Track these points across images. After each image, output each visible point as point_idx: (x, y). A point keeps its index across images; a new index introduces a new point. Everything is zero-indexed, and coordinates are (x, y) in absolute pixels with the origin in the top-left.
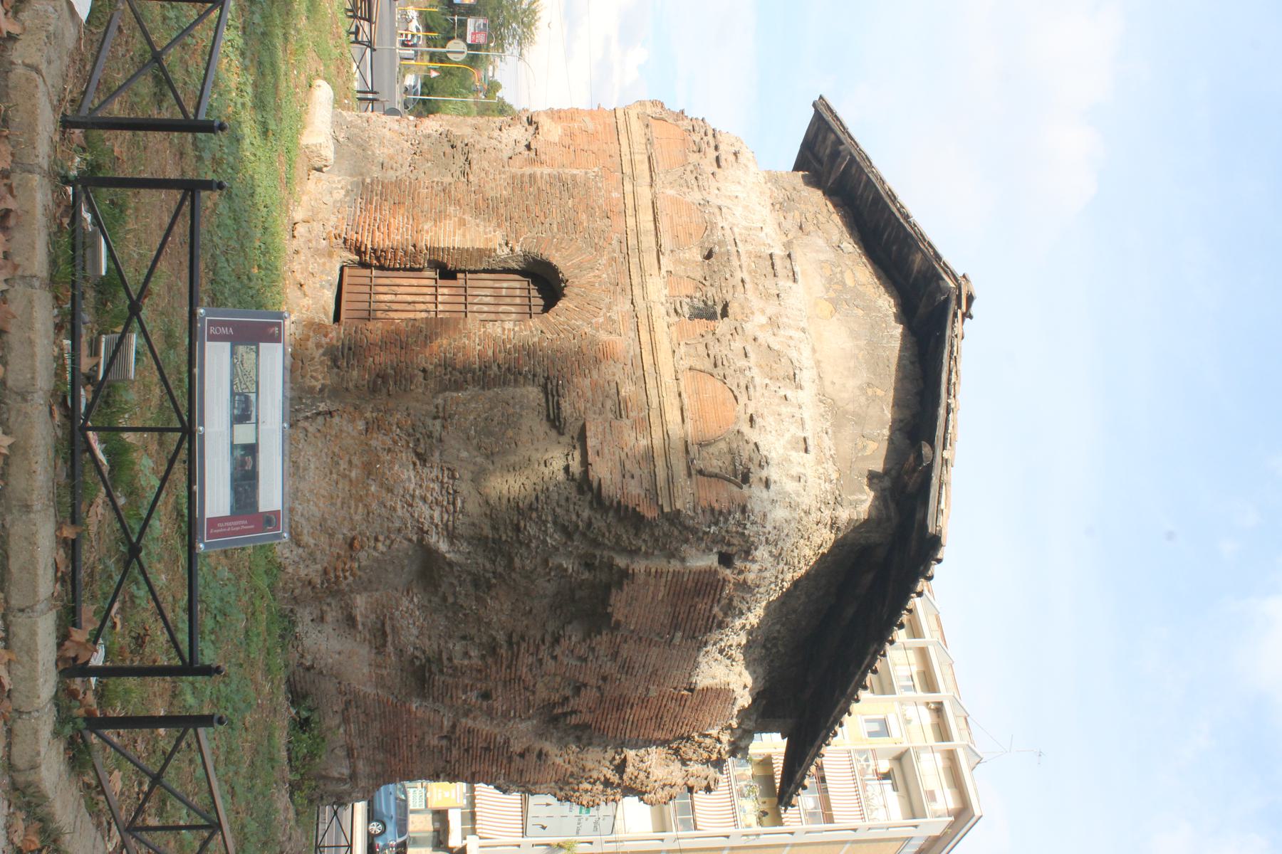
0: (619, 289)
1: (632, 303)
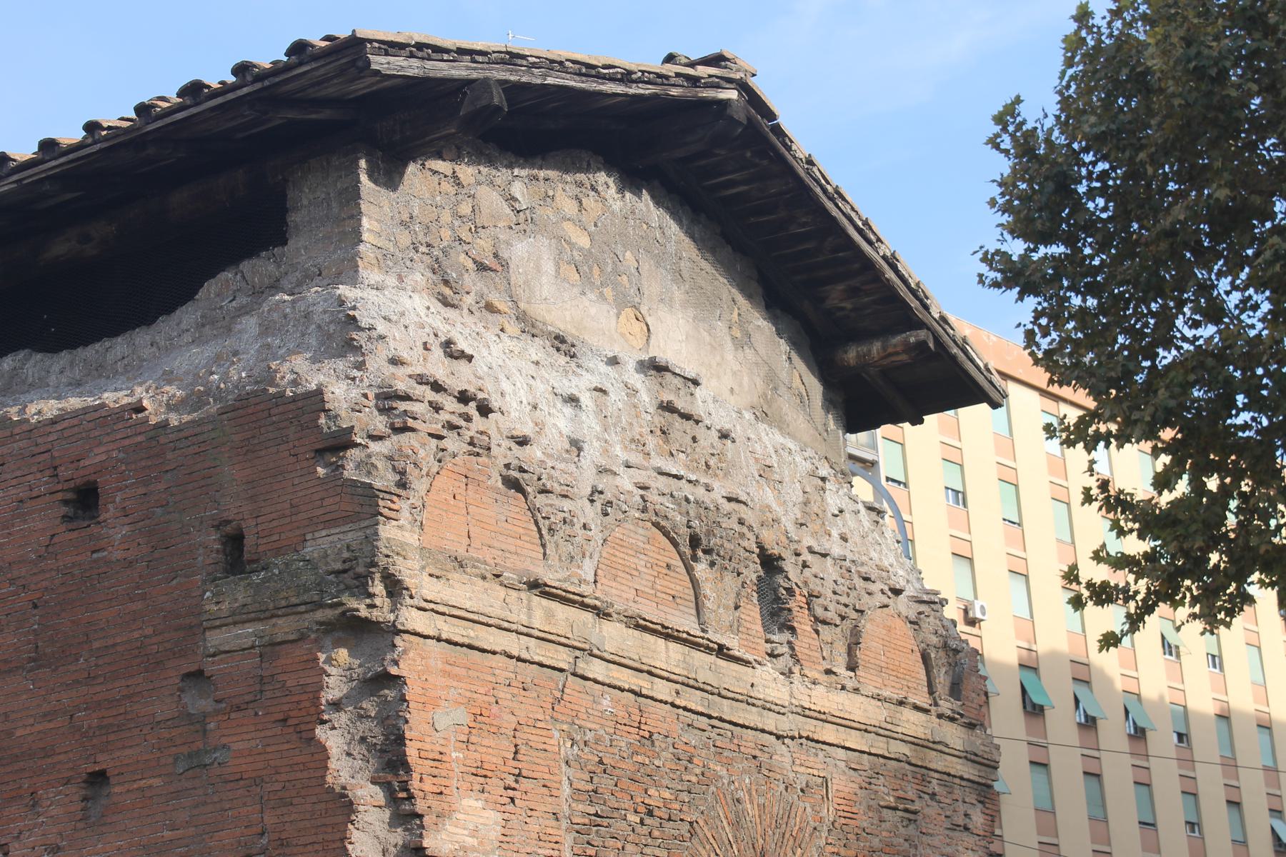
0: (763, 757)
1: (778, 737)
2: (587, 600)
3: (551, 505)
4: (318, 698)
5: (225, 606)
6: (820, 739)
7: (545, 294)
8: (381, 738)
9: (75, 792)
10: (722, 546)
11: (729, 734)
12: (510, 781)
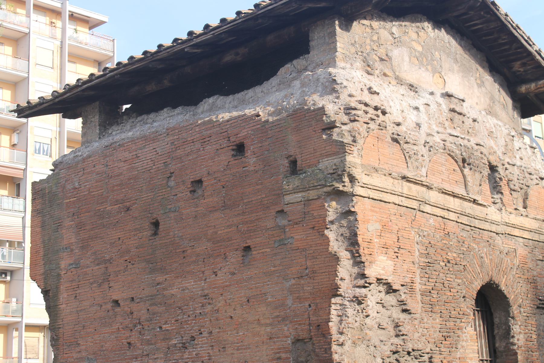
0: (491, 241)
1: (497, 234)
2: (423, 183)
3: (409, 148)
4: (325, 220)
5: (291, 186)
6: (513, 234)
7: (405, 69)
8: (349, 234)
9: (240, 253)
10: (474, 162)
11: (478, 233)
12: (396, 250)
